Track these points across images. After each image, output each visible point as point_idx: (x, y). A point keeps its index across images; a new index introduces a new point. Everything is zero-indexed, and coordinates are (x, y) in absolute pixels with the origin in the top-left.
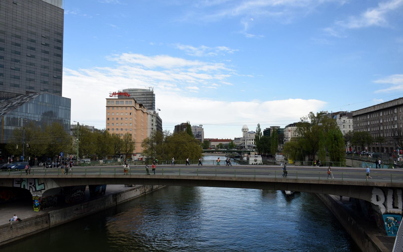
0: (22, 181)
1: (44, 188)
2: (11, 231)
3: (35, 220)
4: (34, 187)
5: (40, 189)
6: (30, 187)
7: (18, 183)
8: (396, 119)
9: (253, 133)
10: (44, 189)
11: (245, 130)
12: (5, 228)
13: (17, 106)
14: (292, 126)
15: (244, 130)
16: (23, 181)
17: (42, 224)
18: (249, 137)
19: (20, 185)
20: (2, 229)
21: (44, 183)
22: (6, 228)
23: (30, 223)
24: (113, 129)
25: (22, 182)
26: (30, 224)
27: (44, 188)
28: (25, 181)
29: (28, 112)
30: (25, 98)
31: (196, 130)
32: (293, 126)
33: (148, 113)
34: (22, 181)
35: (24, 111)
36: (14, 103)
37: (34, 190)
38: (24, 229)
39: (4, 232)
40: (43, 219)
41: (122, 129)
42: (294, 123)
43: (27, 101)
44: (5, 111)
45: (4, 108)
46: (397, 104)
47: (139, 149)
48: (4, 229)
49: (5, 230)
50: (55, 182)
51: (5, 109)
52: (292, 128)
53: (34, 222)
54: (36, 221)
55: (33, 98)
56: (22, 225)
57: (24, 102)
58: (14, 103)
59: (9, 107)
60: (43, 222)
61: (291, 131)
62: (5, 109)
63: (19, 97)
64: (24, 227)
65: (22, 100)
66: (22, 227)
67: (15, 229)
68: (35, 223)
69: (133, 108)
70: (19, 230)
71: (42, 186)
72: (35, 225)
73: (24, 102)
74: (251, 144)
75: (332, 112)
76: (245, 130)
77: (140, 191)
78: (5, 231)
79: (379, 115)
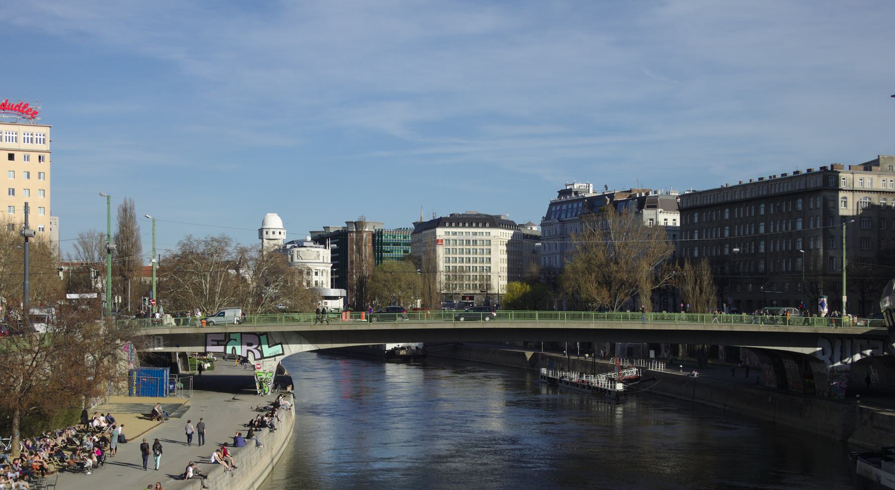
0: (227, 340)
1: (281, 352)
4: (259, 350)
5: (272, 355)
6: (248, 351)
7: (218, 345)
8: (799, 226)
9: (311, 247)
10: (283, 354)
11: (274, 233)
14: (447, 224)
16: (230, 340)
18: (296, 260)
19: (223, 347)
21: (281, 344)
25: (228, 342)
27: (281, 352)
28: (236, 340)
32: (450, 226)
34: (227, 340)
37: (258, 356)
42: (513, 221)
46: (805, 188)
61: (444, 242)
71: (277, 349)
76: (274, 233)
79: (757, 210)
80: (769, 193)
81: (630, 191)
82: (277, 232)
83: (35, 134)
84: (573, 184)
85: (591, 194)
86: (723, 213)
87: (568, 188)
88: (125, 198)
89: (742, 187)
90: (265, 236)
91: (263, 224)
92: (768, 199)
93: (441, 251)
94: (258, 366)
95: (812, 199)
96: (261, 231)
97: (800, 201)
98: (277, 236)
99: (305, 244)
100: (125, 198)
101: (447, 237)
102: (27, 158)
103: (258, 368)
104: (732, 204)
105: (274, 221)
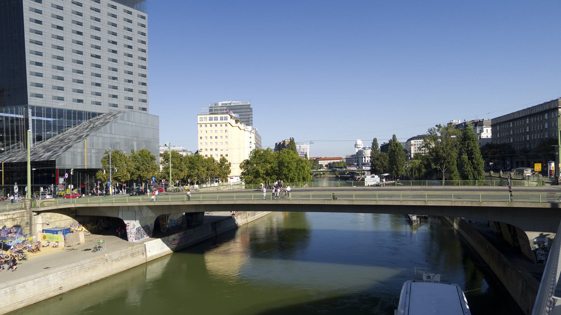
2: (106, 262)
3: (130, 251)
12: (100, 260)
13: (101, 126)
15: (358, 145)
17: (138, 255)
20: (97, 261)
22: (101, 260)
23: (126, 254)
24: (206, 150)
26: (125, 256)
29: (113, 133)
30: (109, 117)
31: (300, 147)
32: (416, 139)
33: (245, 129)
35: (108, 131)
36: (96, 124)
38: (119, 261)
39: (99, 265)
40: (139, 250)
41: (216, 149)
43: (111, 120)
44: (87, 132)
45: (86, 129)
46: (549, 108)
47: (236, 171)
48: (98, 261)
49: (100, 263)
50: (150, 210)
51: (88, 130)
52: (415, 142)
53: (130, 253)
54: (131, 253)
55: (117, 117)
56: (118, 257)
57: (108, 122)
58: (96, 124)
59: (91, 128)
60: (139, 254)
62: (88, 130)
63: (101, 116)
64: (120, 258)
65: (106, 119)
66: (117, 259)
67: (110, 260)
68: (131, 254)
69: (228, 124)
70: (114, 262)
72: (131, 257)
73: (108, 122)
74: (366, 162)
75: (465, 121)
76: (359, 145)
77: (241, 218)
78: (99, 264)
80: (531, 113)
81: (473, 121)
82: (360, 145)
83: (224, 117)
84: (453, 121)
85: (460, 123)
86: (509, 125)
87: (451, 122)
88: (291, 138)
89: (518, 112)
90: (356, 147)
91: (356, 143)
92: (530, 116)
93: (412, 148)
94: (128, 225)
95: (553, 113)
96: (355, 145)
97: (546, 115)
98: (360, 146)
99: (366, 148)
100: (291, 138)
101: (415, 143)
102: (221, 126)
103: (128, 226)
104: (513, 120)
105: (359, 142)
